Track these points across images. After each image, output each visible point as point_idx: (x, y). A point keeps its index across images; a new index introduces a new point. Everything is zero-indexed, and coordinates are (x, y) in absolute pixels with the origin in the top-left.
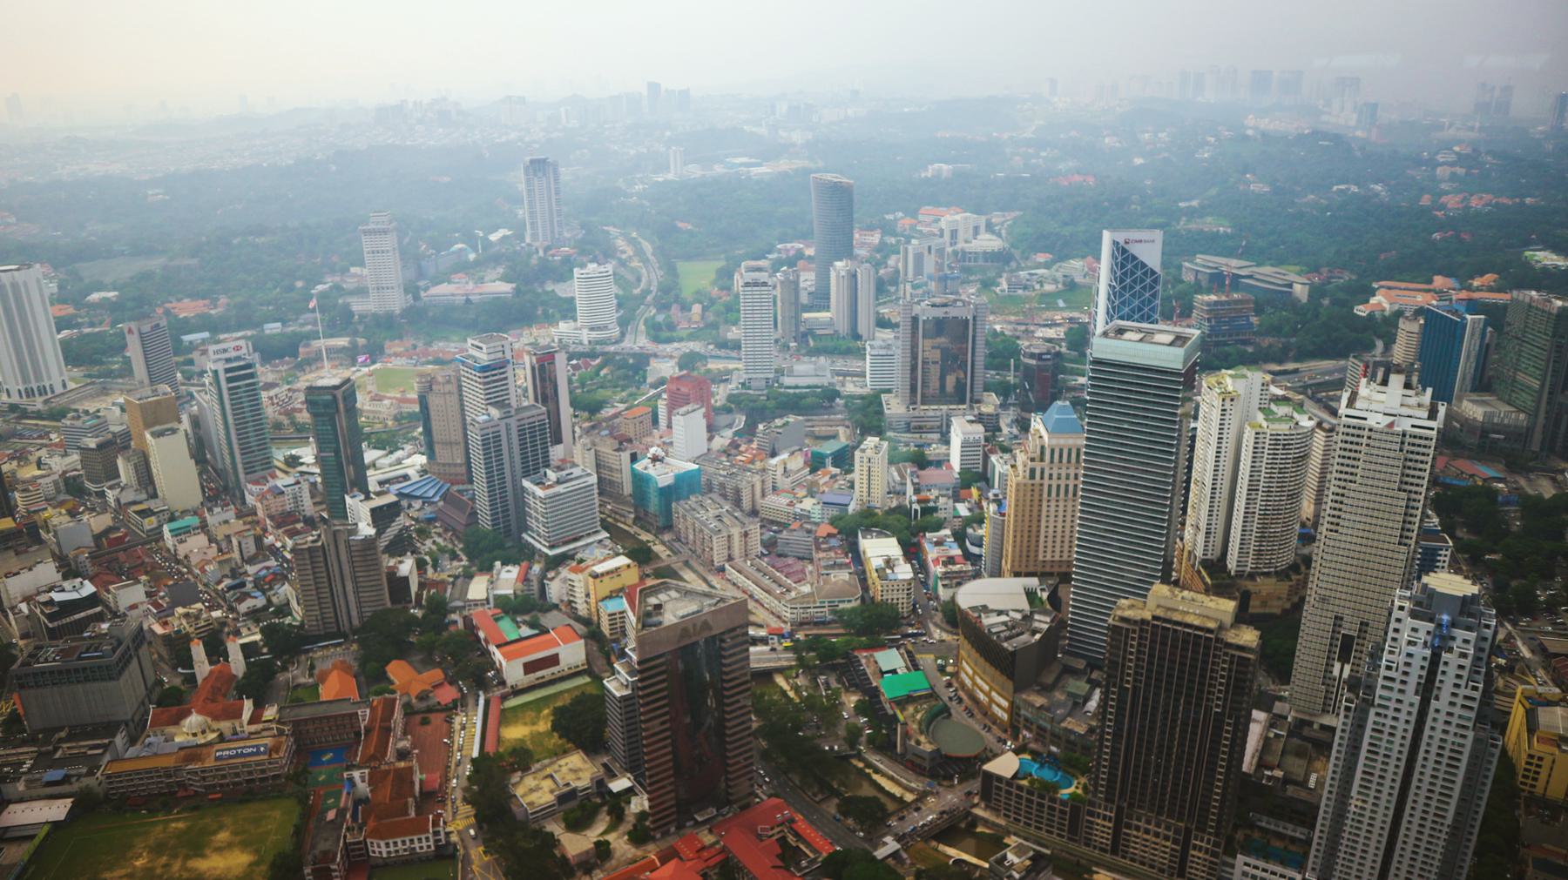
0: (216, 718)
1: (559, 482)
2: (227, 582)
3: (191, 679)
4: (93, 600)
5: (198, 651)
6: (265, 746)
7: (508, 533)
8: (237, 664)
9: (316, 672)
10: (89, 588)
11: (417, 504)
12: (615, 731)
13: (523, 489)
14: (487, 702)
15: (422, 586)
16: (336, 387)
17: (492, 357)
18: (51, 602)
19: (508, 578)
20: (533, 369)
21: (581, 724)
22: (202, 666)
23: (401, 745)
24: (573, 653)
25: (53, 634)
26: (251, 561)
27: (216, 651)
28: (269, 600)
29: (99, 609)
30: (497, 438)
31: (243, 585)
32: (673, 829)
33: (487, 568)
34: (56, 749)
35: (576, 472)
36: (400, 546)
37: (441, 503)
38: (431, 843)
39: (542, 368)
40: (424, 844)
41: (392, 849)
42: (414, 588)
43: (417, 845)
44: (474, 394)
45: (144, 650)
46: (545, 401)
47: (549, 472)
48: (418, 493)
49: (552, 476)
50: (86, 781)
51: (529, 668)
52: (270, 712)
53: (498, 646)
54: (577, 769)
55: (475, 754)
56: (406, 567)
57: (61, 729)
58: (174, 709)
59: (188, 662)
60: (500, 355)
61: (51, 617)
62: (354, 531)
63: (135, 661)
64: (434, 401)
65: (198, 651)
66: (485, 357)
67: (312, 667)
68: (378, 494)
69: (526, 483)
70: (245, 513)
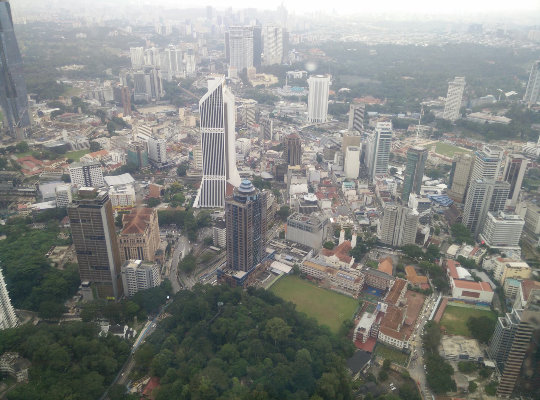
0: (341, 260)
1: (505, 219)
2: (358, 211)
3: (337, 242)
4: (315, 203)
5: (342, 234)
6: (355, 278)
7: (473, 230)
8: (354, 243)
9: (379, 258)
10: (315, 198)
11: (437, 205)
12: (496, 339)
13: (487, 216)
14: (442, 299)
15: (429, 239)
16: (420, 151)
17: (493, 156)
18: (303, 199)
19: (467, 250)
20: (509, 164)
21: (480, 328)
22: (342, 239)
23: (402, 300)
24: (487, 296)
25: (301, 210)
26: (369, 206)
27: (348, 237)
28: (370, 223)
29: (316, 206)
30: (483, 191)
31: (363, 214)
32: (508, 397)
33: (459, 242)
34: (292, 249)
35: (516, 217)
36: (424, 221)
37: (448, 208)
38: (402, 345)
40: (399, 344)
41: (387, 339)
42: (426, 239)
43: (396, 343)
44: (479, 169)
45: (326, 227)
47: (502, 213)
48: (439, 201)
49: (503, 215)
50: (297, 263)
51: (465, 293)
52: (360, 267)
53: (454, 279)
54: (472, 348)
55: (430, 319)
56: (426, 230)
57: (295, 243)
58: (329, 251)
59: (338, 236)
60: (497, 156)
61: (302, 204)
62: (411, 211)
63: (322, 229)
64: (459, 166)
65: (342, 234)
66: (490, 155)
67: (378, 255)
68: (424, 197)
69: (489, 214)
70: (372, 188)
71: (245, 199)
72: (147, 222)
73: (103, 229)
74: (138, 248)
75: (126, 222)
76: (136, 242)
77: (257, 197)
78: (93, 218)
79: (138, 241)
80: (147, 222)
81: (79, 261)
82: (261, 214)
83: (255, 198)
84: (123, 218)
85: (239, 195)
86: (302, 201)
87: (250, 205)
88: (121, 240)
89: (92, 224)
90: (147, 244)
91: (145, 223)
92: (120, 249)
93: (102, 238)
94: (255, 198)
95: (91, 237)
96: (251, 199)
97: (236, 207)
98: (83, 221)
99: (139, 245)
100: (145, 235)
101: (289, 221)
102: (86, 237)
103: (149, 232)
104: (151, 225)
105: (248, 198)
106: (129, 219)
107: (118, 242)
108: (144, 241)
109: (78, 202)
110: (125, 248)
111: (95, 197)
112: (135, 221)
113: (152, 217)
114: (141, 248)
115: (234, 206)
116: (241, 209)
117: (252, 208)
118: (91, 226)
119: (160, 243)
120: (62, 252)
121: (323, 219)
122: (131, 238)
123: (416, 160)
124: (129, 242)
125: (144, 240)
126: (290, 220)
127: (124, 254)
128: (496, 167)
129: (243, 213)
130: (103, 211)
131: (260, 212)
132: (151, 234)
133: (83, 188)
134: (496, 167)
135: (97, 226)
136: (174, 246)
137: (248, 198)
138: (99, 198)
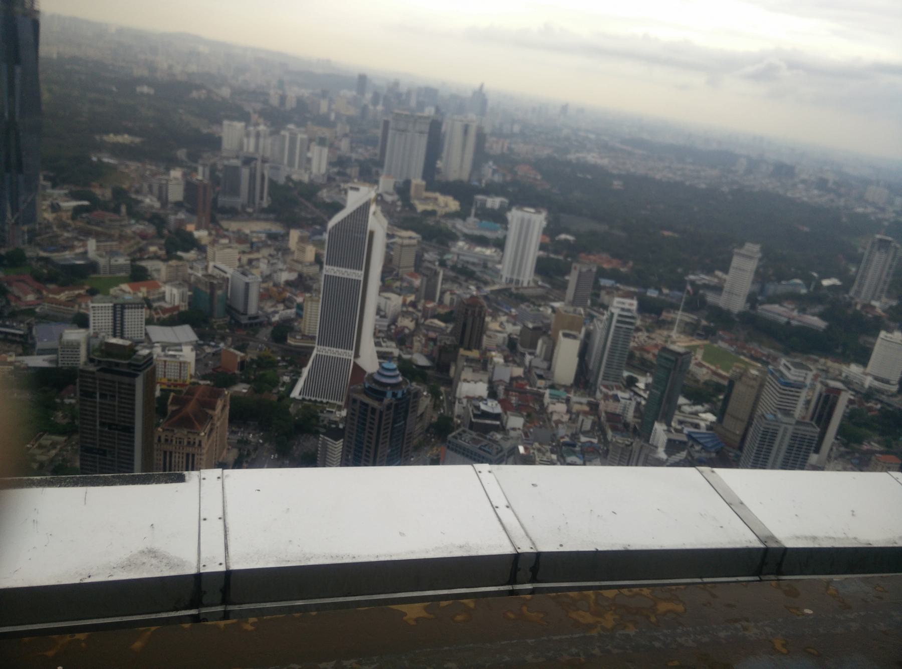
2: (567, 439)
4: (497, 417)
10: (498, 409)
11: (697, 448)
18: (478, 408)
20: (820, 395)
25: (472, 426)
26: (586, 433)
29: (498, 423)
30: (774, 435)
31: (574, 446)
37: (714, 455)
39: (827, 397)
46: (818, 422)
48: (702, 441)
60: (801, 379)
61: (475, 416)
64: (739, 388)
71: (384, 394)
72: (210, 412)
73: (133, 414)
74: (188, 455)
75: (174, 408)
76: (186, 443)
77: (403, 394)
78: (120, 393)
79: (189, 443)
80: (210, 412)
81: (81, 464)
82: (405, 424)
83: (400, 395)
84: (170, 400)
85: (374, 386)
86: (476, 412)
87: (389, 407)
88: (160, 437)
89: (116, 403)
90: (204, 451)
91: (207, 414)
92: (155, 453)
93: (130, 430)
94: (400, 395)
95: (110, 426)
96: (394, 395)
97: (367, 405)
98: (103, 396)
99: (190, 450)
100: (203, 434)
101: (450, 442)
102: (102, 424)
103: (211, 430)
104: (216, 418)
105: (389, 394)
106: (181, 401)
107: (156, 440)
108: (200, 445)
109: (99, 362)
110: (165, 452)
111: (129, 357)
112: (190, 408)
113: (220, 404)
114: (193, 455)
115: (363, 403)
116: (374, 410)
117: (392, 411)
118: (114, 406)
119: (225, 452)
120: (54, 445)
121: (507, 445)
122: (178, 435)
123: (670, 370)
124: (174, 442)
125: (200, 442)
126: (454, 440)
127: (162, 463)
128: (798, 397)
129: (377, 417)
130: (139, 382)
131: (405, 418)
132: (214, 434)
133: (114, 341)
134: (798, 397)
135: (124, 408)
136: (249, 460)
137: (389, 394)
138: (137, 360)
